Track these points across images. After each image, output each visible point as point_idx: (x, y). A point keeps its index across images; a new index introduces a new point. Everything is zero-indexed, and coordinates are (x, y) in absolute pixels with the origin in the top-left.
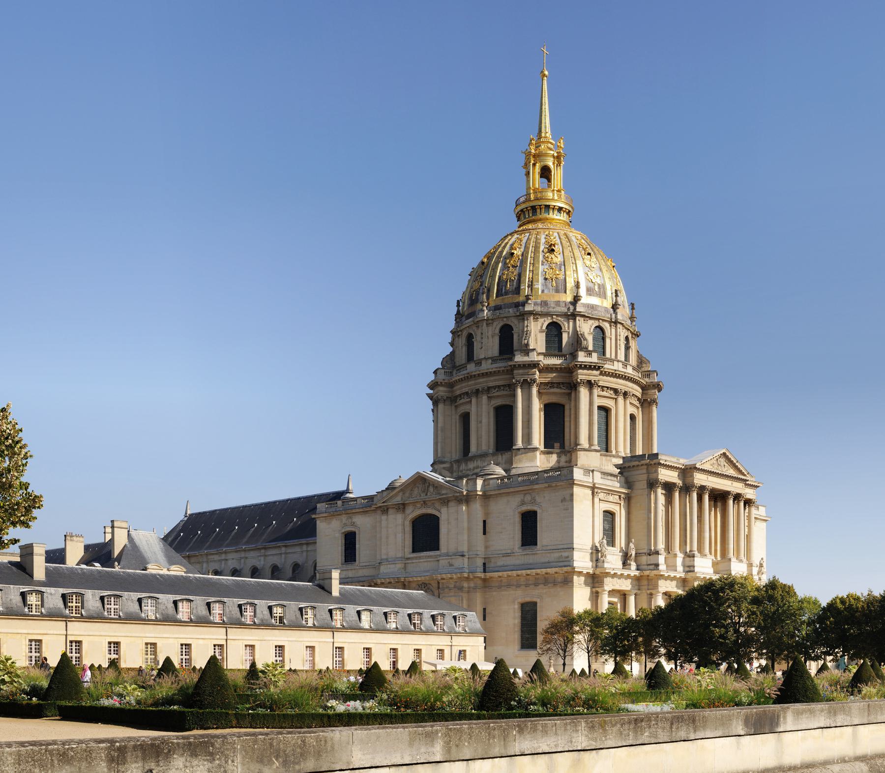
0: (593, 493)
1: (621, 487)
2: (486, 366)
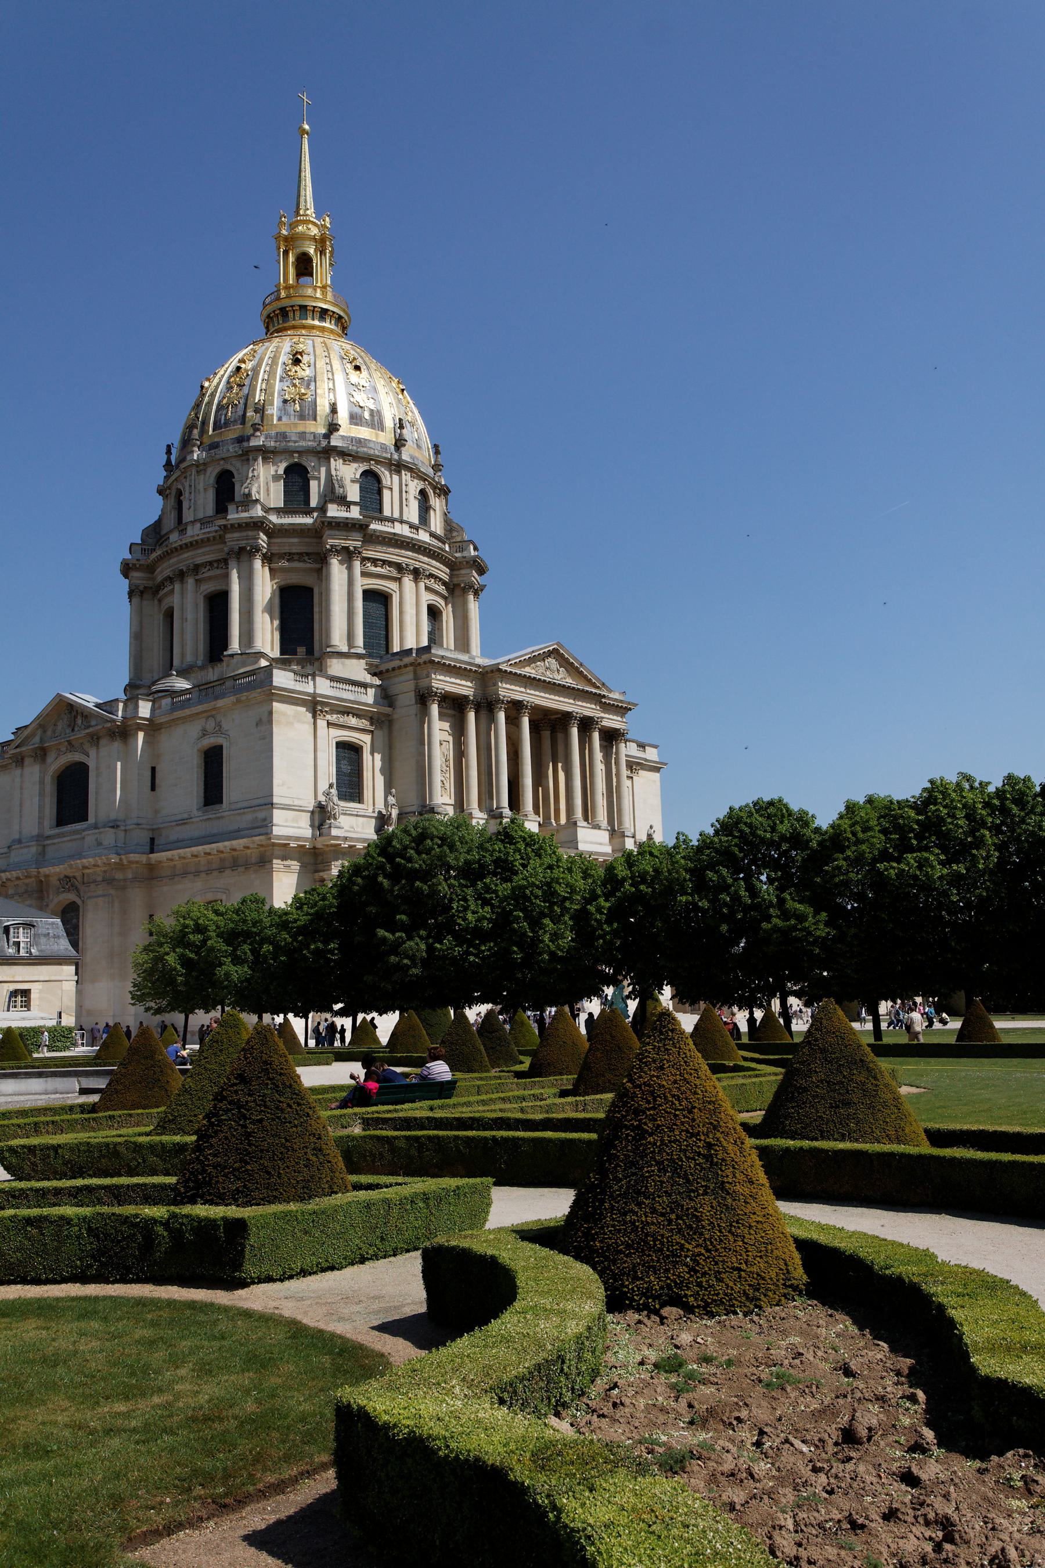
2: (194, 532)
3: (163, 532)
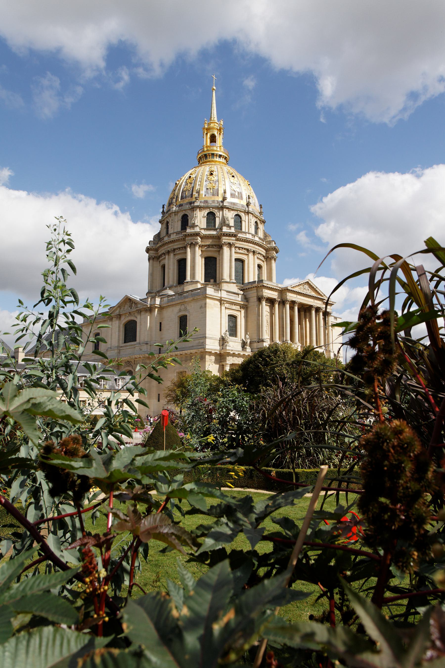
1: (242, 301)
2: (174, 237)
3: (161, 237)
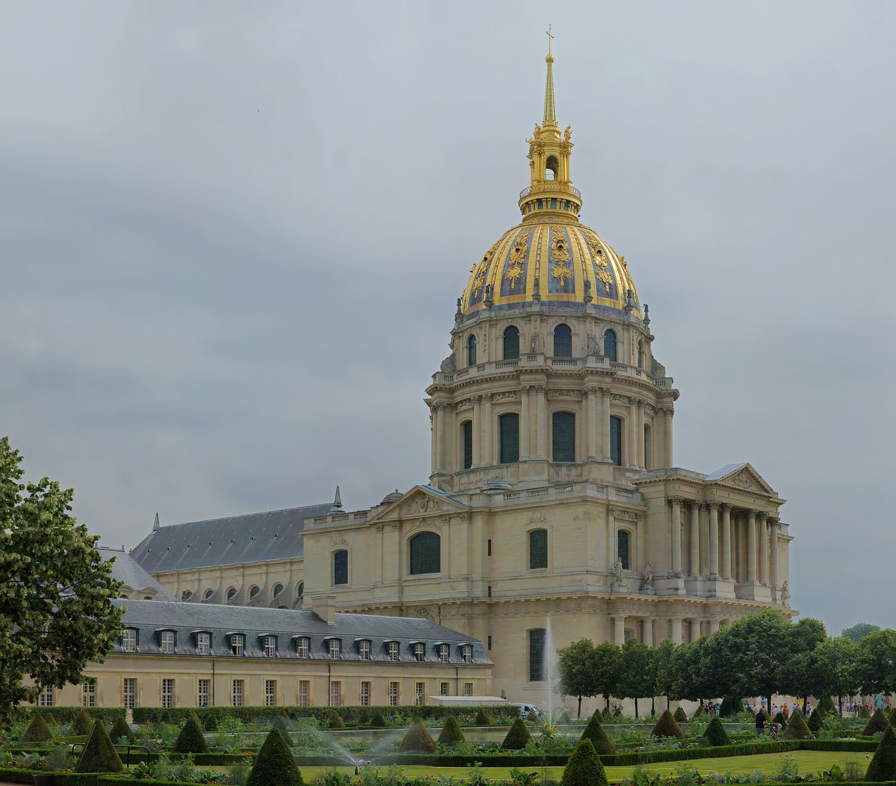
0: (608, 510)
2: (490, 371)
